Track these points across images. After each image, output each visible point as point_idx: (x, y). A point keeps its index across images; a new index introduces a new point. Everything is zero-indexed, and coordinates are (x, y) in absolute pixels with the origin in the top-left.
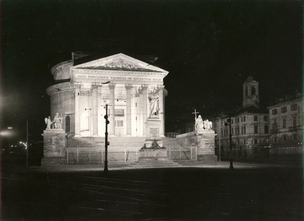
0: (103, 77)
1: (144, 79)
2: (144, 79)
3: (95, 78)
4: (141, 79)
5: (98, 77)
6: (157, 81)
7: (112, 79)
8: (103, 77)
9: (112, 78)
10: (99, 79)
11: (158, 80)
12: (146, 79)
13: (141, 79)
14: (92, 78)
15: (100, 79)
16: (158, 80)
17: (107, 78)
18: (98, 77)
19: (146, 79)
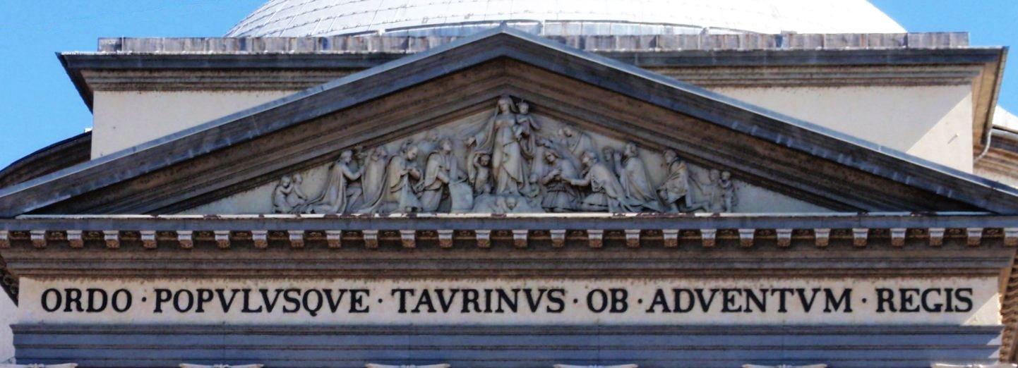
0: (313, 301)
1: (773, 301)
2: (773, 301)
3: (226, 308)
4: (741, 301)
5: (256, 300)
6: (923, 317)
8: (313, 301)
9: (411, 302)
10: (264, 318)
11: (933, 299)
12: (793, 301)
13: (741, 301)
14: (192, 317)
15: (277, 317)
16: (933, 299)
17: (355, 301)
18: (256, 300)
19: (793, 301)
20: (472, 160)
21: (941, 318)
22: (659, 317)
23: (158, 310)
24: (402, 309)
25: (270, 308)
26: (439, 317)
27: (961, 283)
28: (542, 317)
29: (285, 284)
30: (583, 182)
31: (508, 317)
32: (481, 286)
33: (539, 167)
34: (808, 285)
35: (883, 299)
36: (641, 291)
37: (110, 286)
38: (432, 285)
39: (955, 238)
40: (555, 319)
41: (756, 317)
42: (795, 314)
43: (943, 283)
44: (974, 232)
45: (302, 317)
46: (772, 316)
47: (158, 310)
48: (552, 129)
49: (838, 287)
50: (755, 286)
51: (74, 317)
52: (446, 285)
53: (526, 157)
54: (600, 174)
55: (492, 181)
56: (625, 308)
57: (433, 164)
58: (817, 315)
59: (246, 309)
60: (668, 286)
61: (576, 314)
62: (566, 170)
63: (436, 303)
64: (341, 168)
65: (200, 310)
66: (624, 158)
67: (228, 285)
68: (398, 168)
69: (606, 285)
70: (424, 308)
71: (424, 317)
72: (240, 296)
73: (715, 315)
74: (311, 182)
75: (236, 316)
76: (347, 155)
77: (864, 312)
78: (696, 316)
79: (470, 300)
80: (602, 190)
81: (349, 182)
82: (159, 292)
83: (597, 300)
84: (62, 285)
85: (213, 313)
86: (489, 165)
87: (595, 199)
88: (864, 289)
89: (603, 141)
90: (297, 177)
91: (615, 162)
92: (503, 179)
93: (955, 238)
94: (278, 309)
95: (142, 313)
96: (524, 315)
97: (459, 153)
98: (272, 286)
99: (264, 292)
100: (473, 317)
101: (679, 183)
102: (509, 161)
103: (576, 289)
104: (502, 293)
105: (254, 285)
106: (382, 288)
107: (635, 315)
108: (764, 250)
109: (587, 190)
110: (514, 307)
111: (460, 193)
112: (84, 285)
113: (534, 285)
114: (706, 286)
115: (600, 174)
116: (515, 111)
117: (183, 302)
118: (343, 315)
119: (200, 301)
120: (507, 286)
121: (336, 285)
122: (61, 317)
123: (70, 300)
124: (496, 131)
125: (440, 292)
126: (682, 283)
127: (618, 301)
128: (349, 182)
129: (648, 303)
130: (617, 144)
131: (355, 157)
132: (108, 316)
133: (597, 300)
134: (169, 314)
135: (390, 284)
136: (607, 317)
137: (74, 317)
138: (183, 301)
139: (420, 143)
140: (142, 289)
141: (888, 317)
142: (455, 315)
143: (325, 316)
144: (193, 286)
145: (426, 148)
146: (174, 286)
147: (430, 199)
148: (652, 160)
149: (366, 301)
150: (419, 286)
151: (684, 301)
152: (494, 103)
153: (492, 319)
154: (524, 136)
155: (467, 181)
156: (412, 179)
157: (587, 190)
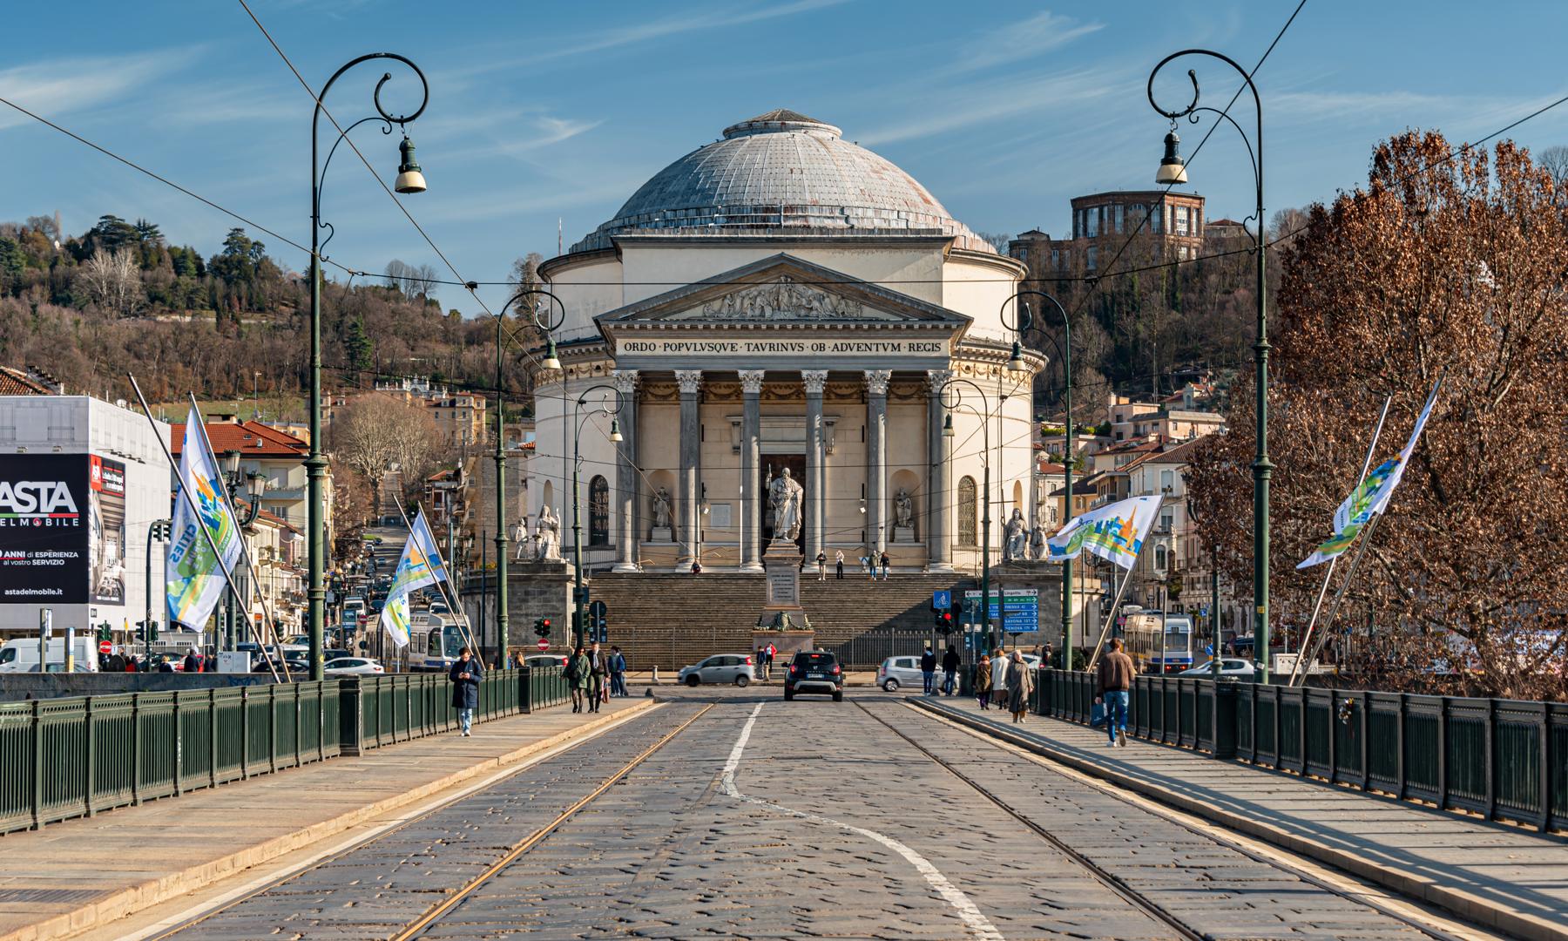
6: (924, 354)
15: (706, 353)
22: (836, 353)
26: (761, 353)
28: (796, 353)
31: (785, 353)
34: (885, 342)
35: (911, 347)
36: (829, 343)
37: (648, 341)
38: (759, 341)
41: (868, 353)
42: (882, 352)
44: (942, 326)
45: (714, 353)
46: (874, 353)
48: (800, 287)
49: (896, 342)
50: (868, 342)
51: (636, 353)
52: (764, 341)
53: (790, 297)
54: (816, 304)
58: (889, 353)
60: (839, 342)
61: (808, 352)
67: (689, 341)
68: (747, 302)
69: (818, 341)
71: (756, 353)
73: (855, 353)
74: (716, 305)
75: (692, 352)
77: (905, 352)
78: (848, 353)
79: (771, 347)
84: (632, 341)
85: (684, 351)
88: (905, 343)
89: (817, 290)
91: (821, 299)
95: (659, 351)
96: (790, 353)
98: (704, 341)
100: (773, 353)
101: (842, 307)
102: (784, 298)
103: (808, 343)
105: (698, 341)
106: (741, 342)
107: (828, 352)
108: (872, 329)
112: (639, 341)
113: (794, 341)
114: (852, 342)
115: (816, 304)
118: (729, 352)
119: (679, 347)
120: (784, 341)
121: (726, 341)
122: (631, 353)
123: (634, 347)
127: (822, 347)
132: (648, 353)
134: (669, 352)
136: (818, 353)
137: (636, 353)
139: (754, 291)
140: (659, 342)
141: (913, 353)
142: (767, 352)
143: (722, 352)
144: (677, 341)
146: (670, 341)
147: (757, 312)
148: (833, 298)
150: (754, 341)
153: (779, 353)
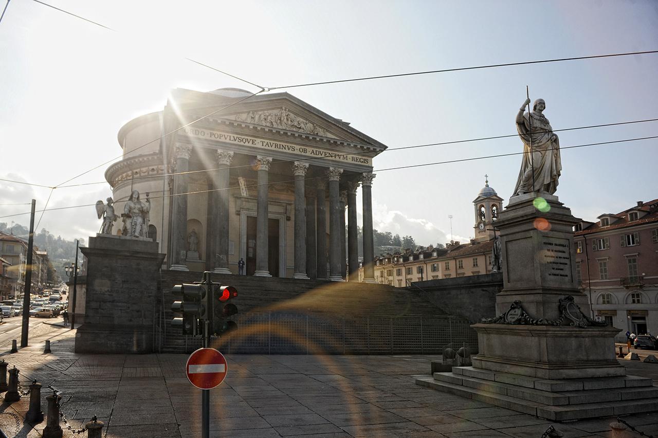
3: (226, 139)
5: (232, 138)
6: (360, 163)
7: (263, 147)
9: (264, 144)
10: (234, 142)
13: (328, 155)
16: (362, 160)
20: (277, 118)
21: (362, 164)
22: (313, 155)
23: (211, 137)
24: (263, 145)
25: (235, 140)
27: (367, 158)
28: (290, 151)
29: (239, 136)
30: (299, 127)
31: (284, 150)
32: (279, 143)
33: (289, 122)
35: (353, 159)
36: (309, 150)
38: (269, 141)
39: (368, 149)
40: (293, 152)
43: (364, 158)
45: (242, 143)
47: (211, 137)
52: (272, 142)
53: (287, 120)
55: (281, 123)
56: (306, 152)
57: (269, 117)
59: (230, 140)
60: (315, 150)
61: (297, 152)
62: (296, 124)
63: (269, 144)
64: (251, 115)
65: (220, 138)
66: (306, 124)
69: (303, 147)
70: (267, 146)
72: (229, 137)
76: (251, 112)
80: (303, 129)
81: (252, 118)
82: (211, 133)
83: (301, 150)
86: (280, 120)
87: (301, 131)
90: (241, 115)
92: (283, 123)
93: (368, 149)
94: (237, 141)
97: (274, 116)
99: (234, 137)
100: (277, 149)
104: (283, 146)
107: (308, 154)
109: (300, 128)
110: (285, 149)
111: (274, 123)
113: (289, 145)
116: (285, 110)
117: (216, 136)
119: (220, 136)
120: (284, 144)
124: (282, 113)
125: (270, 143)
126: (317, 150)
127: (305, 151)
128: (252, 118)
129: (311, 152)
130: (305, 121)
131: (253, 113)
133: (301, 150)
135: (262, 140)
136: (303, 154)
138: (216, 136)
143: (247, 144)
145: (267, 114)
149: (255, 142)
150: (266, 141)
151: (317, 152)
152: (281, 108)
154: (287, 115)
155: (276, 122)
156: (265, 119)
157: (300, 128)
